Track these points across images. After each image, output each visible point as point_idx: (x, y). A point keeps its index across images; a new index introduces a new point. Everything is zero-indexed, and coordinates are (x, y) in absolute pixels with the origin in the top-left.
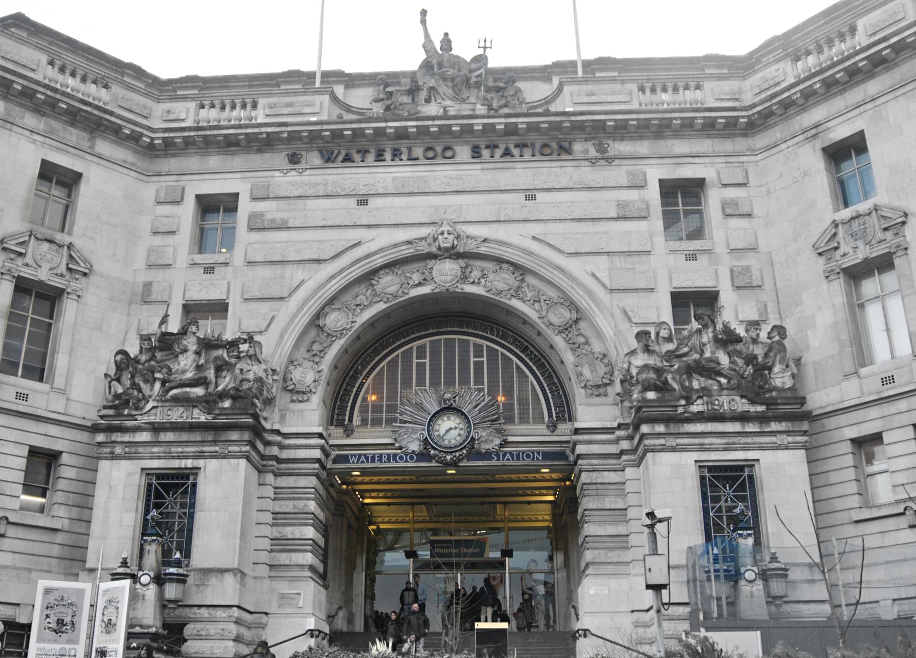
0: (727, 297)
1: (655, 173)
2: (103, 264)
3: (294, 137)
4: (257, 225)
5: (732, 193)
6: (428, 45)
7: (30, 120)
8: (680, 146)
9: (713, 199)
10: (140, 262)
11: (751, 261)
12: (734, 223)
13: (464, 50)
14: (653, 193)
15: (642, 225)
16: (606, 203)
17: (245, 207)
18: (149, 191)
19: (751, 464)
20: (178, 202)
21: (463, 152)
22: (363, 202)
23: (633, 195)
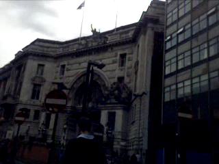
0: (126, 77)
1: (119, 53)
2: (47, 79)
3: (71, 54)
4: (68, 70)
5: (130, 55)
6: (92, 31)
7: (35, 58)
8: (124, 47)
9: (127, 56)
10: (53, 78)
11: (130, 70)
12: (130, 62)
13: (97, 31)
14: (118, 57)
15: (115, 64)
16: (110, 60)
17: (67, 66)
18: (56, 65)
19: (115, 113)
20: (58, 67)
21: (93, 53)
22: (80, 64)
23: (114, 58)
